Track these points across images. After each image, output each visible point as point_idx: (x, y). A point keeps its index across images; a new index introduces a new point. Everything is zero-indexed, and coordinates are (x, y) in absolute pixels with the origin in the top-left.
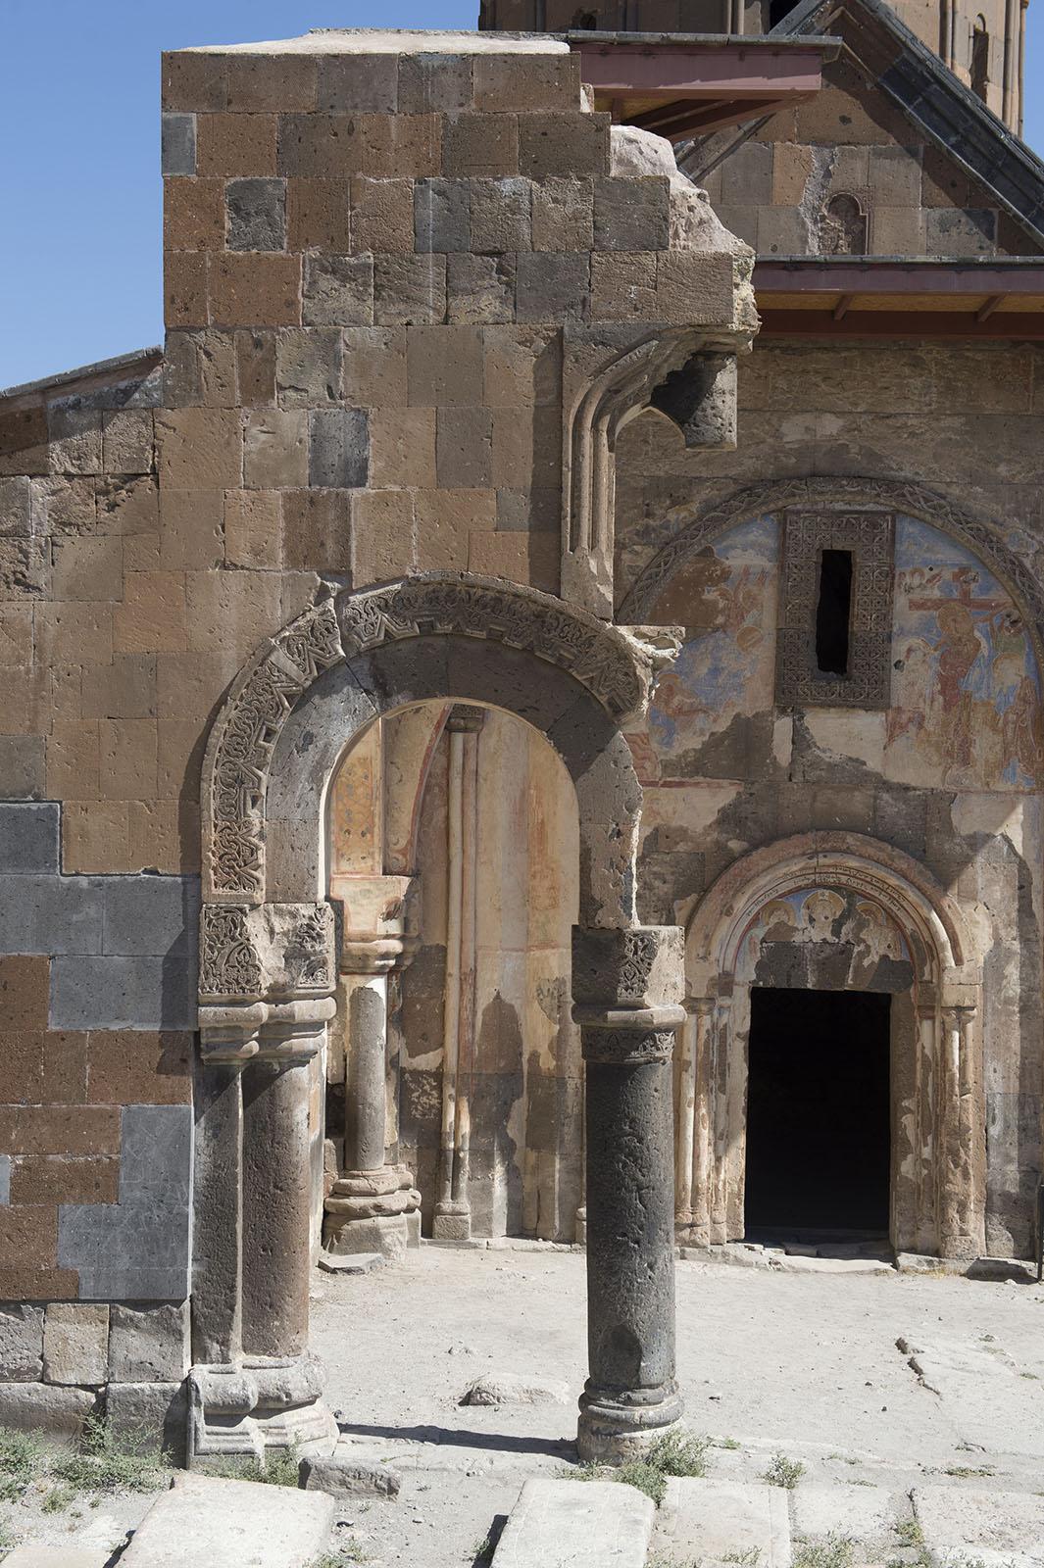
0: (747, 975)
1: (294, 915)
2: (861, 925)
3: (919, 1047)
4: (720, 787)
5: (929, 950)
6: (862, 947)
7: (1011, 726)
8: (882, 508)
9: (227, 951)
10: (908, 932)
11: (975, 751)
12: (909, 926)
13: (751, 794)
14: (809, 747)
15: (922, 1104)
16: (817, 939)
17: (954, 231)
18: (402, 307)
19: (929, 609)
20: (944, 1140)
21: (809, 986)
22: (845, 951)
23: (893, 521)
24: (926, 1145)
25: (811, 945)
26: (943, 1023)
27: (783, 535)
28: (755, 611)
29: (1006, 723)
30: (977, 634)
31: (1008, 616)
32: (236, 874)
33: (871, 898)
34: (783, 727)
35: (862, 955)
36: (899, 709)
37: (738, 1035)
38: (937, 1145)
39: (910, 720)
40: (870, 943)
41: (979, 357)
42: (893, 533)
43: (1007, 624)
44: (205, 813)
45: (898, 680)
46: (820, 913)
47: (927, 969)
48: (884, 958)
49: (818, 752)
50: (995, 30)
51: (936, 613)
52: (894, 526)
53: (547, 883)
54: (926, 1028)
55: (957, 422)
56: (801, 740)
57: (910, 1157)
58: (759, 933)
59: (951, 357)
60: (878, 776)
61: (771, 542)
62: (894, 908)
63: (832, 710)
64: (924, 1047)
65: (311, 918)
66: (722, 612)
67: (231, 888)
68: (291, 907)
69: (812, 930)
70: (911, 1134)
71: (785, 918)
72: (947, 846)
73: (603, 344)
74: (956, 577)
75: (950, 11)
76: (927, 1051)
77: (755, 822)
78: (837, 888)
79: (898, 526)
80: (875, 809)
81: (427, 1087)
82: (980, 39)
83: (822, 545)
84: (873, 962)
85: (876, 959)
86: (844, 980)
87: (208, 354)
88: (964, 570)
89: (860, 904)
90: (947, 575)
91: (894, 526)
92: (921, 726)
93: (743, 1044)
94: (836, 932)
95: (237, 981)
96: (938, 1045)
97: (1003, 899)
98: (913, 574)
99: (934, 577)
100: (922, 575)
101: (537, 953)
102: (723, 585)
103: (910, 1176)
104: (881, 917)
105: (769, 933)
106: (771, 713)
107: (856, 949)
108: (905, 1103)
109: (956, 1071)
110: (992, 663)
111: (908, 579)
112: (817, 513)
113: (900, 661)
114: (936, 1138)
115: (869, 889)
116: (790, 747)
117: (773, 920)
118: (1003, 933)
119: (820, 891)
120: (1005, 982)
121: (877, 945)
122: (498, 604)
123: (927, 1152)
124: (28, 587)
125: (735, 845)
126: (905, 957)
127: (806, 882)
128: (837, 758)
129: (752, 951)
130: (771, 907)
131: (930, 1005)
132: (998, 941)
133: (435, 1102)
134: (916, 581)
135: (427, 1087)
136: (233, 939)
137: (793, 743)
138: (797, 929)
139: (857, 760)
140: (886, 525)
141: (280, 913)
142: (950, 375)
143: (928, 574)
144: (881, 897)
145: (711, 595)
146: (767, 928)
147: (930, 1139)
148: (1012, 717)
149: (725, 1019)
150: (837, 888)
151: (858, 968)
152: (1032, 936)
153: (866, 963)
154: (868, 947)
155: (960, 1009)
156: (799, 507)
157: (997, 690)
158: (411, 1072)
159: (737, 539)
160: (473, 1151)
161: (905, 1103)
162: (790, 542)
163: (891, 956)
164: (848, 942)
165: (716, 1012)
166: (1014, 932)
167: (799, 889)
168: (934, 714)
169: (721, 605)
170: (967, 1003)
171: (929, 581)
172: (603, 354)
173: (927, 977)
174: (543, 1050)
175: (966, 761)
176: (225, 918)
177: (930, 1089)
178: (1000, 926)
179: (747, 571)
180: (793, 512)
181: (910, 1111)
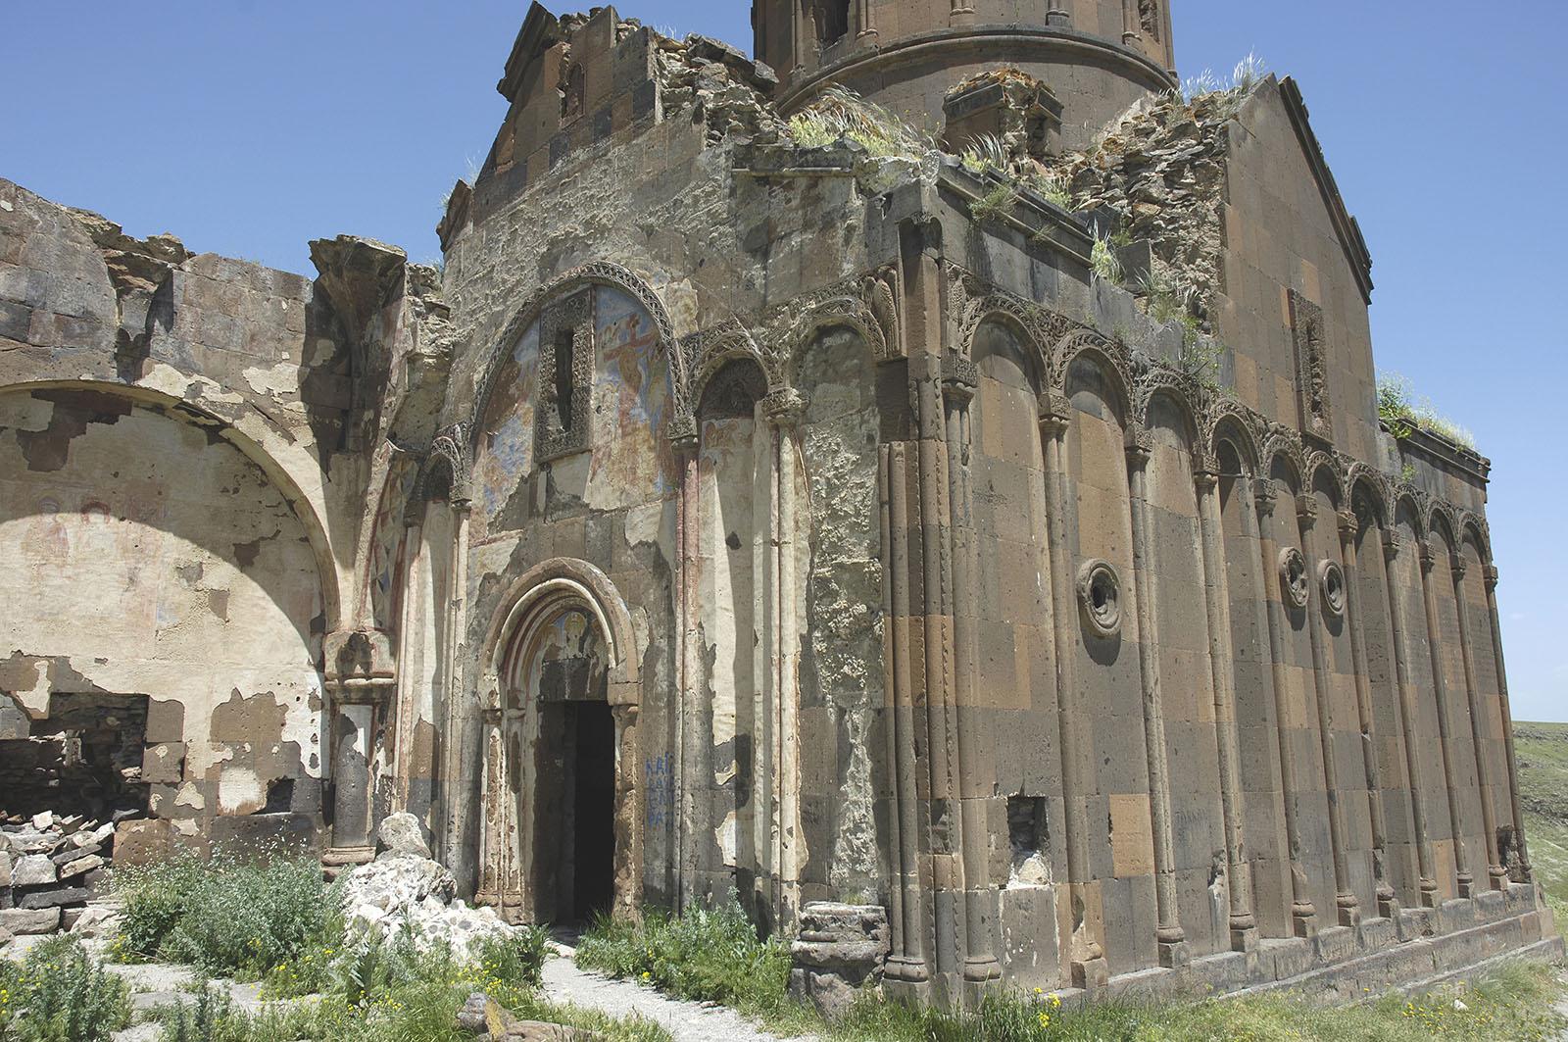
0: (535, 690)
30: (640, 368)
35: (596, 665)
56: (550, 489)
58: (541, 654)
60: (587, 505)
74: (628, 324)
80: (585, 535)
88: (632, 317)
90: (623, 326)
94: (581, 649)
105: (546, 655)
117: (549, 643)
143: (613, 328)
149: (516, 727)
165: (504, 722)
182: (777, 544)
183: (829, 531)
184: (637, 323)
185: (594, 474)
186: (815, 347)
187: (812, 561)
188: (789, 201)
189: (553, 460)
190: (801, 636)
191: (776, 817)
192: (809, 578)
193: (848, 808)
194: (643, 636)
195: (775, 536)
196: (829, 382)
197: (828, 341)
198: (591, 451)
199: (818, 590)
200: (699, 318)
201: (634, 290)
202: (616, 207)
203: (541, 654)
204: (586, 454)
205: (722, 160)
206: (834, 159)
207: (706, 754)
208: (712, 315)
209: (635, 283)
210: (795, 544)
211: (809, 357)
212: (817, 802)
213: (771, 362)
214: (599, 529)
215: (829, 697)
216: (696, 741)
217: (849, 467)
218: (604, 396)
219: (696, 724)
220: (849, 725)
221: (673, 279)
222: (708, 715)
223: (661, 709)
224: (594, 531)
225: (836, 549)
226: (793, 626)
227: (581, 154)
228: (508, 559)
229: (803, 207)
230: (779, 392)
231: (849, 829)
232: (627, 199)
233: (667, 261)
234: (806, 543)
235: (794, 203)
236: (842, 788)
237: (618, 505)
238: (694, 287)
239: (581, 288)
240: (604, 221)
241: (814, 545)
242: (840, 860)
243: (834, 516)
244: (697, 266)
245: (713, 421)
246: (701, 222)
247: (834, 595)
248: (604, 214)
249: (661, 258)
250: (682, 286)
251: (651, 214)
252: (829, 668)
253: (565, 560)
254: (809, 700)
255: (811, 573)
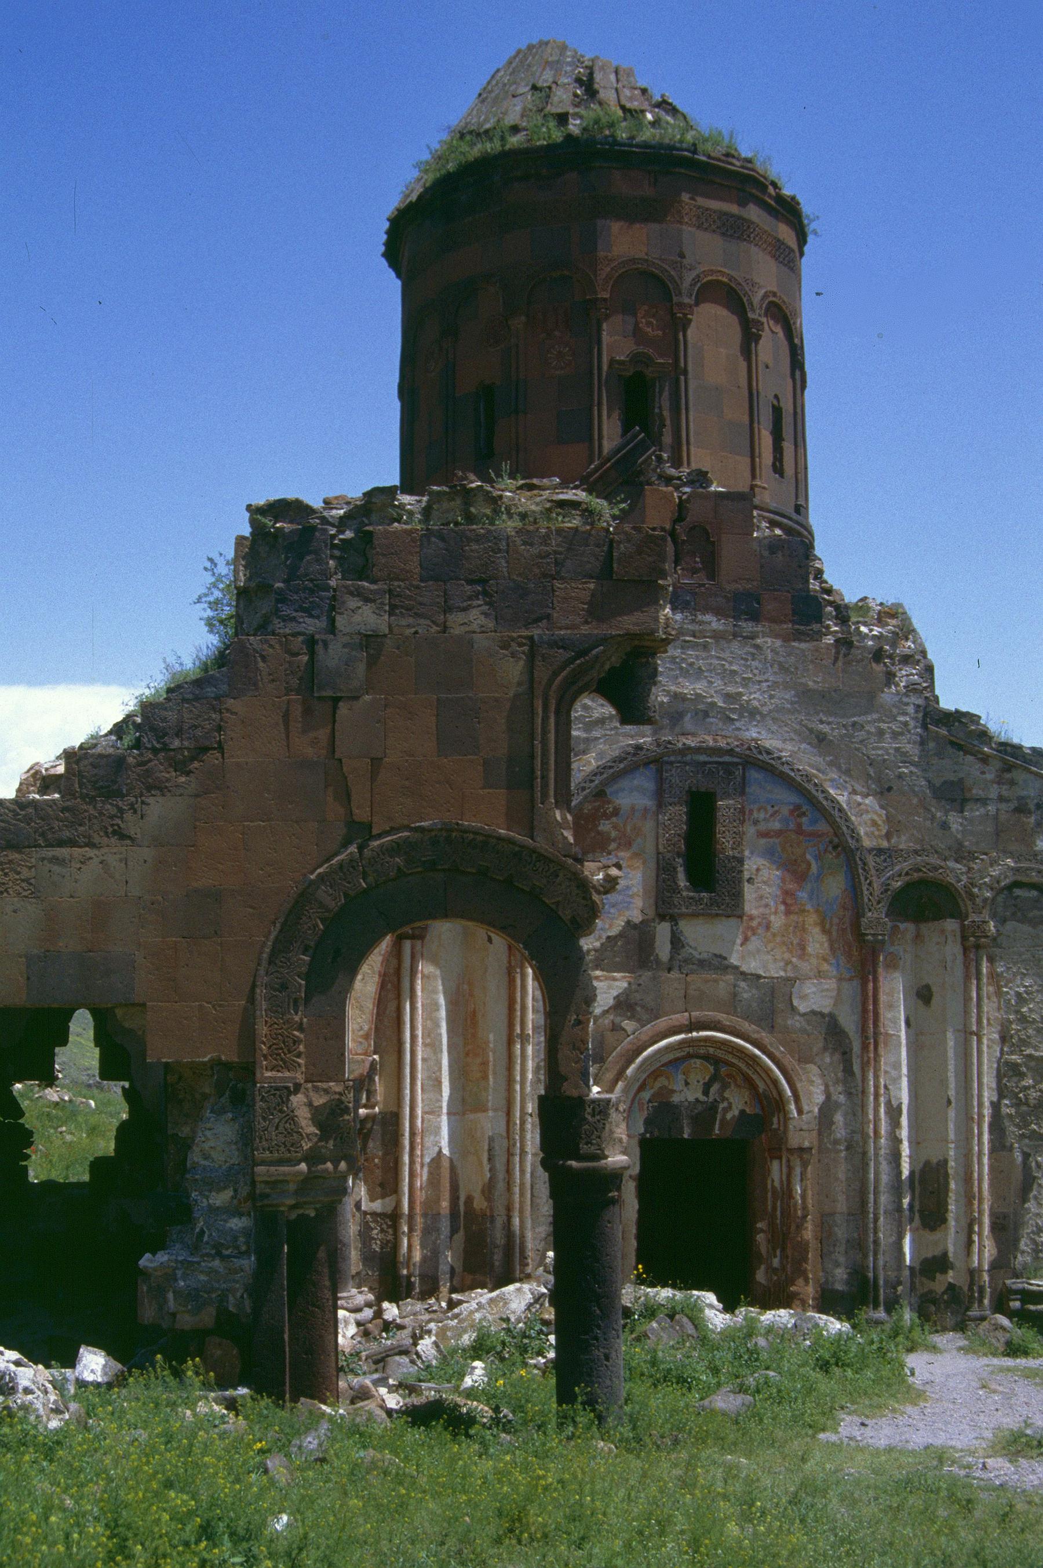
1: (326, 1091)
2: (724, 1087)
3: (769, 1182)
4: (614, 979)
5: (778, 1104)
6: (725, 1104)
7: (835, 927)
8: (736, 760)
9: (277, 1121)
10: (761, 1091)
11: (810, 950)
12: (761, 1086)
13: (639, 985)
14: (683, 946)
15: (772, 1224)
16: (691, 1099)
17: (780, 554)
18: (411, 620)
19: (771, 837)
20: (789, 1252)
21: (686, 1136)
22: (713, 1108)
23: (744, 769)
24: (775, 1256)
25: (686, 1104)
26: (788, 1161)
27: (660, 780)
28: (639, 840)
29: (831, 925)
30: (808, 857)
31: (831, 842)
32: (282, 1059)
33: (732, 1065)
34: (663, 930)
35: (726, 1110)
36: (751, 918)
37: (631, 1177)
38: (784, 1256)
39: (759, 924)
40: (731, 1100)
41: (803, 646)
42: (744, 778)
43: (830, 848)
44: (258, 1013)
45: (749, 892)
46: (692, 1078)
47: (775, 1120)
48: (742, 1112)
49: (691, 950)
50: (787, 406)
51: (777, 841)
52: (744, 773)
53: (479, 1060)
54: (775, 1165)
55: (788, 695)
56: (677, 942)
57: (763, 1267)
58: (646, 1095)
59: (781, 646)
60: (737, 968)
61: (650, 785)
62: (750, 1073)
63: (701, 918)
64: (773, 1181)
65: (340, 1094)
66: (614, 840)
67: (278, 1071)
68: (324, 1085)
69: (687, 1092)
70: (763, 1250)
71: (666, 1083)
72: (789, 1022)
73: (563, 647)
74: (792, 812)
75: (755, 392)
76: (777, 1184)
77: (643, 1007)
78: (706, 1058)
79: (747, 774)
80: (735, 995)
81: (384, 1226)
82: (777, 411)
83: (690, 787)
84: (734, 1116)
85: (737, 1113)
86: (713, 1129)
87: (264, 658)
88: (798, 807)
89: (723, 1070)
90: (785, 811)
91: (744, 773)
92: (768, 927)
93: (634, 1184)
94: (706, 1093)
95: (284, 1143)
96: (784, 1178)
97: (831, 1064)
98: (759, 810)
99: (776, 812)
100: (766, 810)
101: (472, 1116)
102: (614, 819)
103: (763, 1282)
104: (740, 1080)
106: (653, 920)
107: (721, 1106)
108: (759, 1225)
109: (798, 1197)
110: (819, 878)
111: (755, 815)
112: (686, 763)
113: (750, 878)
114: (783, 1250)
115: (730, 1058)
116: (668, 947)
117: (658, 1085)
118: (832, 1089)
119: (692, 1061)
120: (834, 1127)
121: (737, 1102)
122: (486, 843)
123: (776, 1262)
124: (122, 836)
125: (628, 1025)
126: (758, 1111)
127: (683, 1054)
128: (704, 956)
129: (641, 1109)
130: (655, 1075)
131: (778, 1147)
132: (828, 1096)
133: (390, 1237)
134: (762, 815)
135: (384, 1226)
136: (281, 1111)
137: (672, 943)
138: (673, 1091)
139: (720, 956)
140: (739, 772)
141: (316, 1089)
142: (782, 659)
143: (770, 811)
144: (740, 1064)
145: (605, 826)
146: (652, 1091)
147: (778, 1252)
148: (836, 920)
150: (706, 1058)
151: (723, 1119)
152: (853, 1090)
153: (729, 1116)
154: (730, 1104)
155: (801, 1150)
156: (672, 759)
157: (824, 899)
158: (370, 1214)
159: (625, 783)
160: (422, 1277)
161: (759, 1225)
162: (666, 786)
163: (748, 1111)
164: (715, 1100)
166: (840, 1089)
167: (677, 1059)
168: (778, 921)
169: (614, 834)
170: (806, 1144)
171: (771, 816)
172: (563, 655)
173: (775, 1126)
174: (477, 1195)
175: (803, 954)
176: (274, 1095)
177: (778, 1213)
178: (830, 1083)
179: (633, 809)
180: (667, 763)
181: (762, 1231)
182: (976, 1035)
183: (1019, 1030)
184: (804, 814)
185: (746, 939)
186: (1005, 892)
187: (1002, 1050)
188: (983, 773)
189: (683, 916)
190: (992, 1103)
191: (976, 1229)
192: (999, 1062)
193: (1031, 1218)
194: (818, 1091)
195: (974, 1028)
196: (1018, 921)
197: (1017, 892)
198: (740, 917)
199: (1007, 1072)
200: (888, 836)
201: (810, 787)
202: (771, 697)
203: (646, 1095)
204: (733, 921)
205: (911, 709)
206: (1031, 760)
207: (893, 1187)
208: (903, 838)
209: (809, 781)
210: (991, 1034)
211: (1000, 899)
212: (1005, 1217)
213: (972, 897)
214: (754, 991)
215: (1016, 1145)
216: (884, 1178)
217: (1036, 987)
218: (758, 870)
219: (884, 1167)
220: (1033, 1164)
221: (854, 792)
222: (895, 1157)
223: (841, 1151)
224: (747, 992)
225: (1024, 1042)
226: (988, 1096)
227: (714, 623)
228: (611, 1002)
229: (999, 783)
230: (984, 922)
231: (1033, 1232)
232: (788, 695)
233: (848, 772)
234: (996, 1036)
235: (989, 777)
236: (1026, 1206)
237: (782, 974)
238: (882, 807)
239: (727, 759)
240: (755, 703)
241: (1004, 1039)
242: (1023, 1252)
243: (1023, 1019)
244: (884, 791)
245: (899, 924)
246: (888, 754)
247: (1022, 1076)
248: (754, 697)
249: (839, 768)
250: (867, 801)
251: (822, 722)
252: (1017, 1126)
253: (721, 1017)
254: (999, 1145)
255: (1001, 1058)
